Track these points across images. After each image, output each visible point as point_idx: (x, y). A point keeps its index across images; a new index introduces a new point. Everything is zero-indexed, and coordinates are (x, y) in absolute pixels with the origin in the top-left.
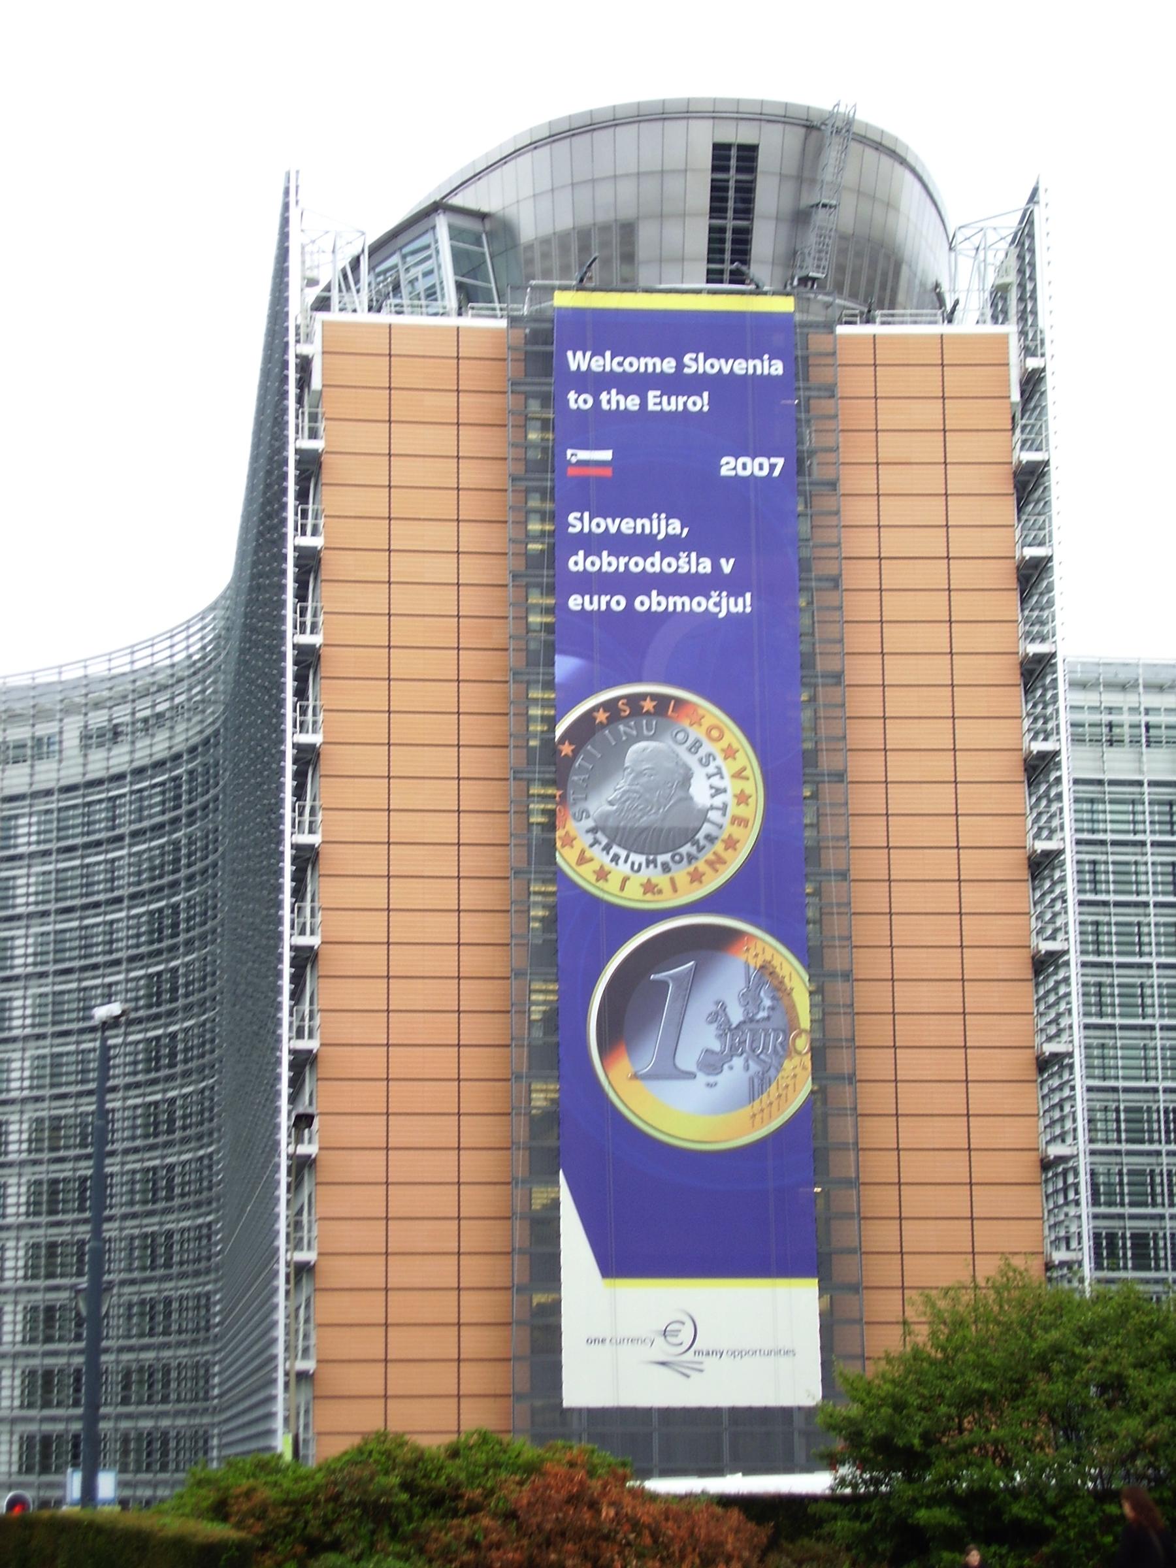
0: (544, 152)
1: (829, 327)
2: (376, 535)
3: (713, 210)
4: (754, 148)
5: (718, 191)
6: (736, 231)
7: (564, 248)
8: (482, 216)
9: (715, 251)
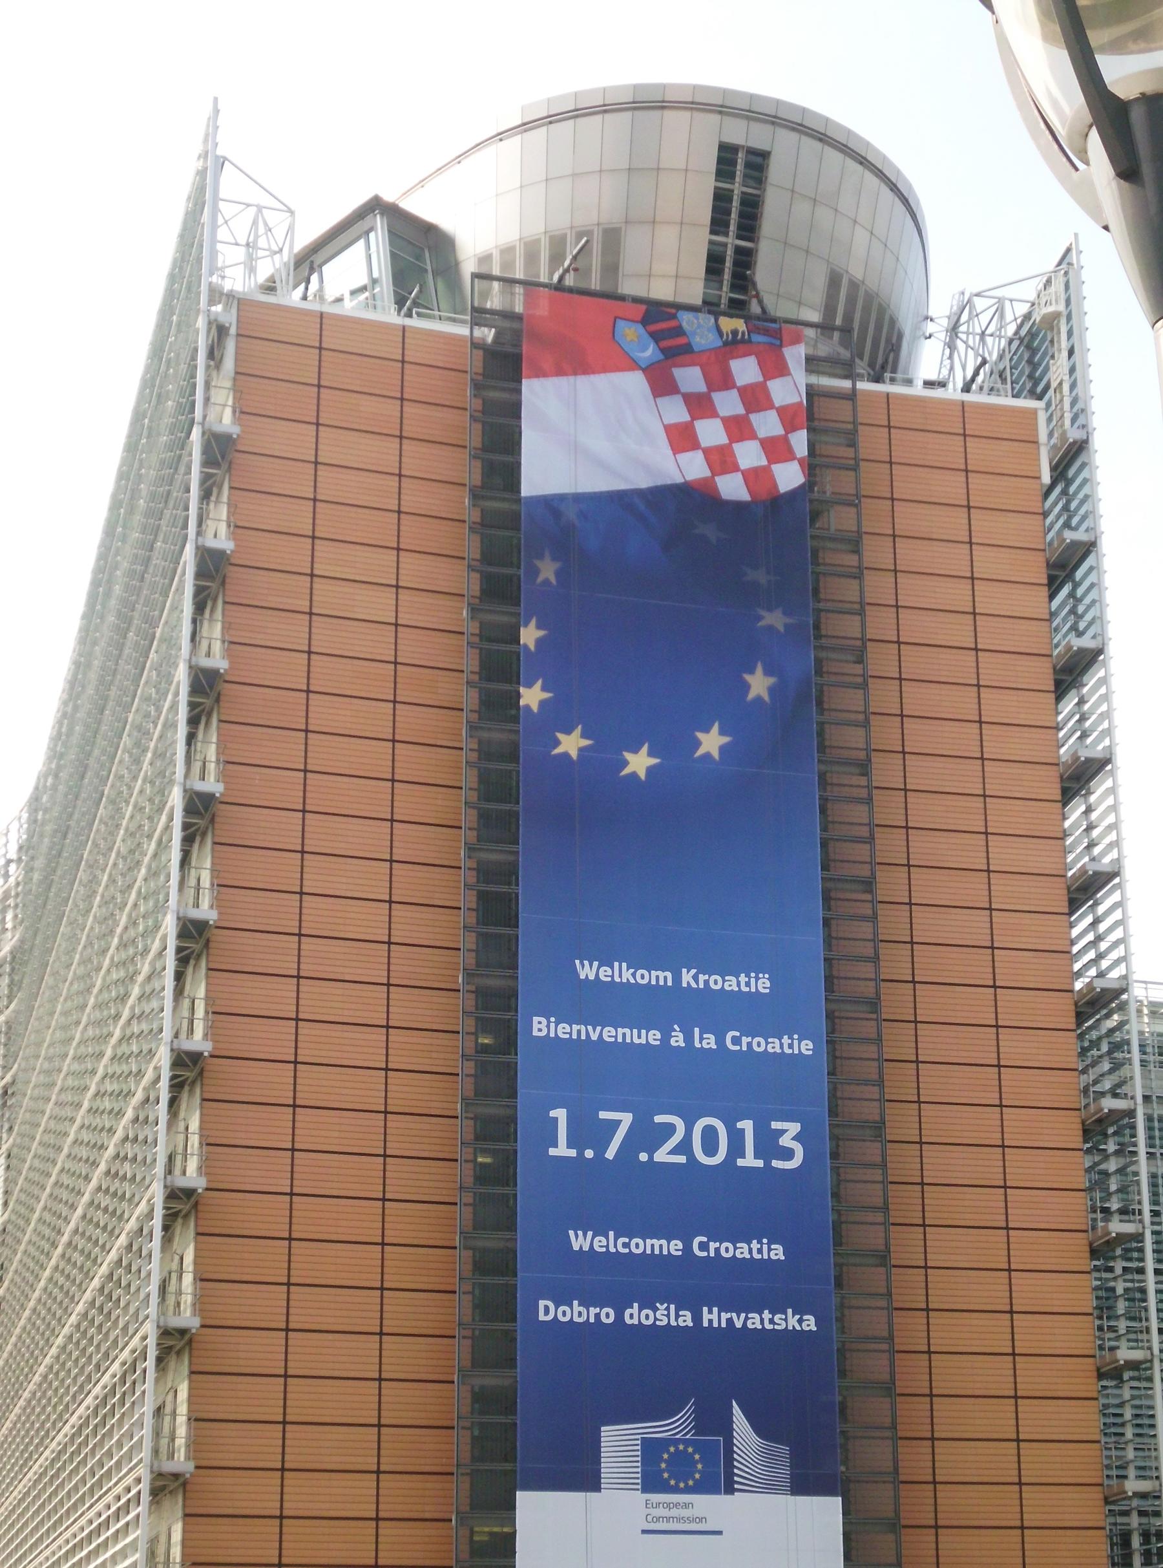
0: (515, 141)
2: (296, 554)
3: (714, 222)
4: (765, 155)
5: (721, 199)
6: (739, 250)
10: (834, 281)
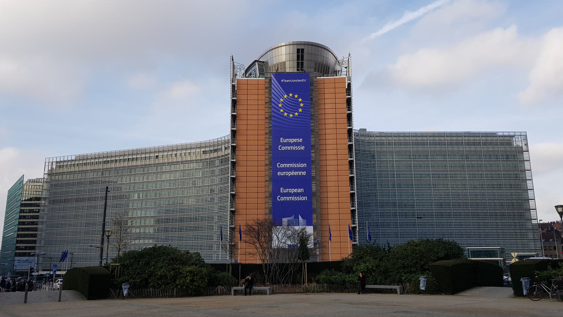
1: (316, 77)
5: (298, 56)
7: (275, 66)
8: (263, 62)
9: (298, 66)
10: (316, 64)
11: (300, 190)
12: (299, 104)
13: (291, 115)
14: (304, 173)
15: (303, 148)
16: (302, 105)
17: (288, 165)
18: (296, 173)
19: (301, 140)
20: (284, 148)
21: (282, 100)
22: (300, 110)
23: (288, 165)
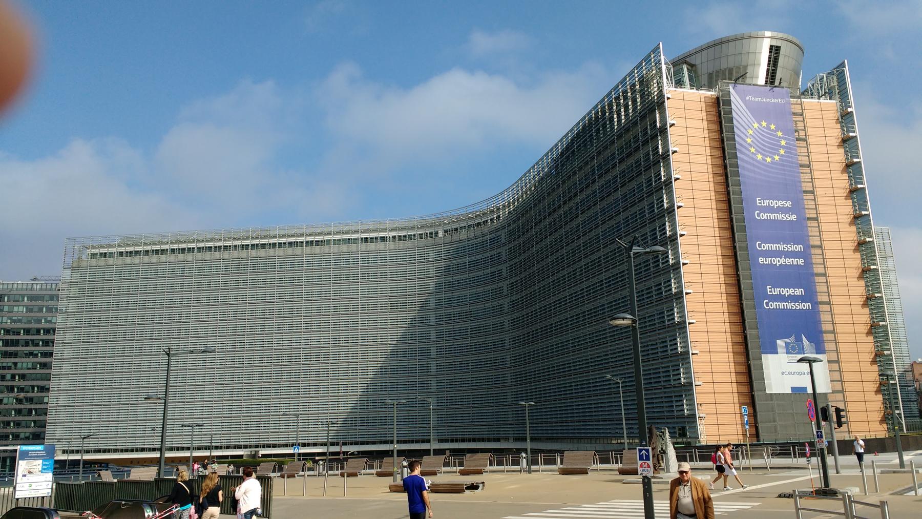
11: (799, 292)
12: (778, 141)
13: (769, 160)
14: (801, 262)
15: (793, 217)
16: (783, 143)
17: (774, 247)
18: (788, 261)
19: (788, 204)
20: (764, 216)
21: (751, 132)
22: (782, 152)
23: (774, 247)
